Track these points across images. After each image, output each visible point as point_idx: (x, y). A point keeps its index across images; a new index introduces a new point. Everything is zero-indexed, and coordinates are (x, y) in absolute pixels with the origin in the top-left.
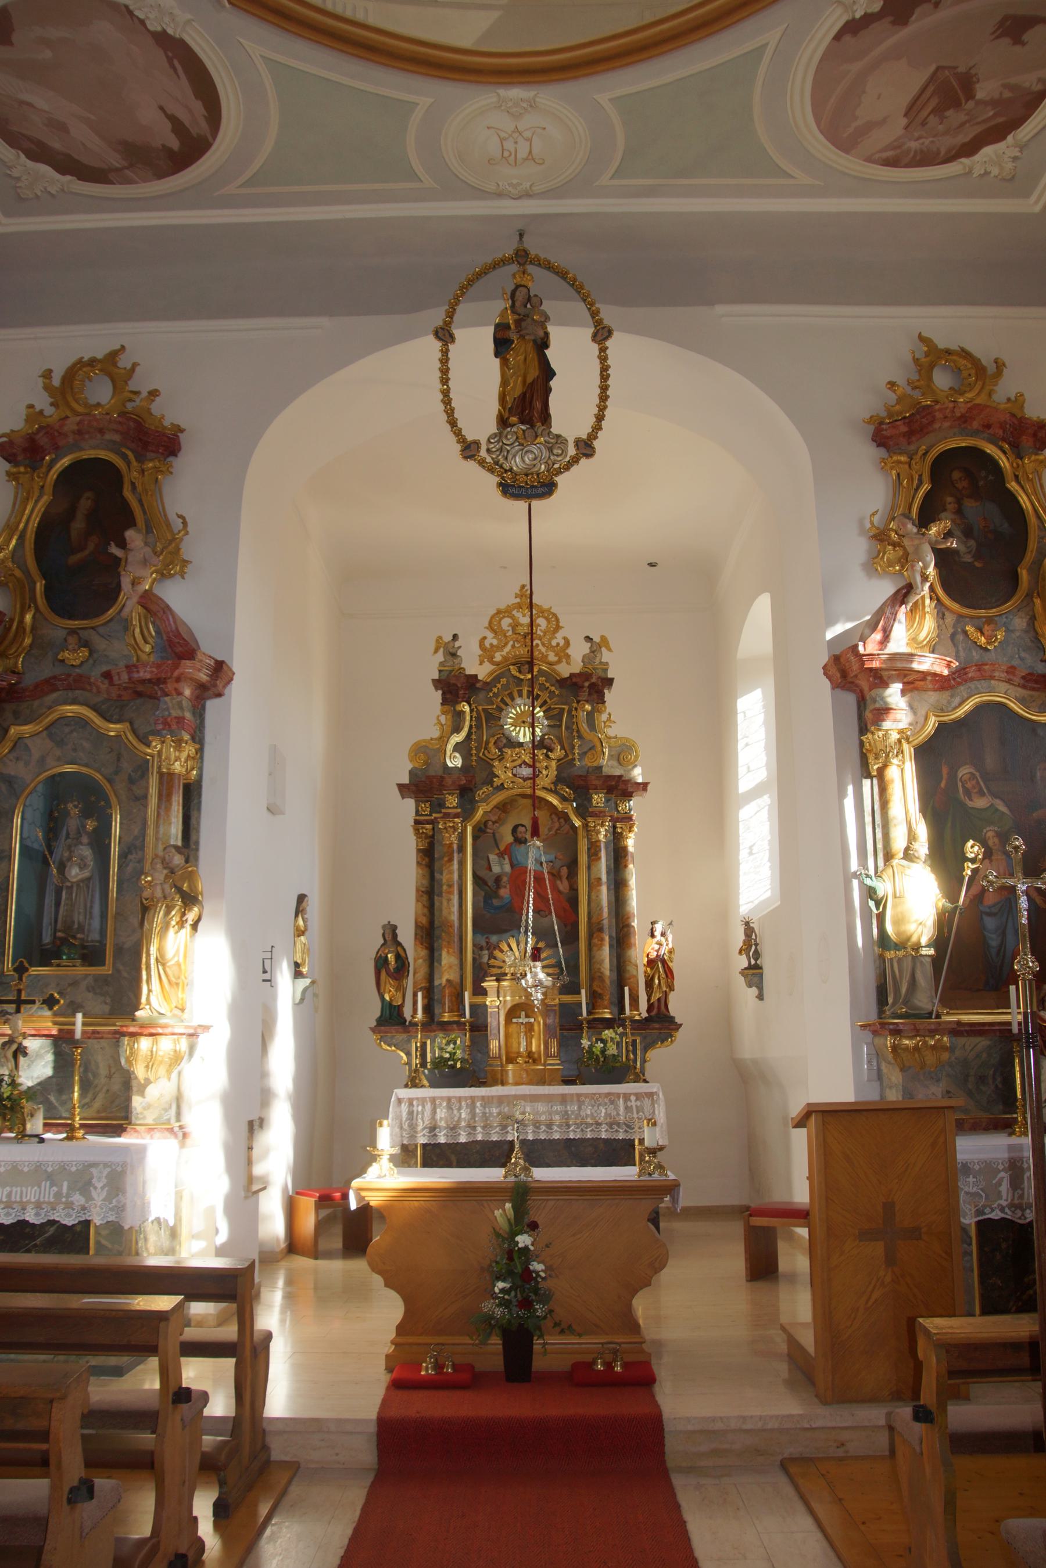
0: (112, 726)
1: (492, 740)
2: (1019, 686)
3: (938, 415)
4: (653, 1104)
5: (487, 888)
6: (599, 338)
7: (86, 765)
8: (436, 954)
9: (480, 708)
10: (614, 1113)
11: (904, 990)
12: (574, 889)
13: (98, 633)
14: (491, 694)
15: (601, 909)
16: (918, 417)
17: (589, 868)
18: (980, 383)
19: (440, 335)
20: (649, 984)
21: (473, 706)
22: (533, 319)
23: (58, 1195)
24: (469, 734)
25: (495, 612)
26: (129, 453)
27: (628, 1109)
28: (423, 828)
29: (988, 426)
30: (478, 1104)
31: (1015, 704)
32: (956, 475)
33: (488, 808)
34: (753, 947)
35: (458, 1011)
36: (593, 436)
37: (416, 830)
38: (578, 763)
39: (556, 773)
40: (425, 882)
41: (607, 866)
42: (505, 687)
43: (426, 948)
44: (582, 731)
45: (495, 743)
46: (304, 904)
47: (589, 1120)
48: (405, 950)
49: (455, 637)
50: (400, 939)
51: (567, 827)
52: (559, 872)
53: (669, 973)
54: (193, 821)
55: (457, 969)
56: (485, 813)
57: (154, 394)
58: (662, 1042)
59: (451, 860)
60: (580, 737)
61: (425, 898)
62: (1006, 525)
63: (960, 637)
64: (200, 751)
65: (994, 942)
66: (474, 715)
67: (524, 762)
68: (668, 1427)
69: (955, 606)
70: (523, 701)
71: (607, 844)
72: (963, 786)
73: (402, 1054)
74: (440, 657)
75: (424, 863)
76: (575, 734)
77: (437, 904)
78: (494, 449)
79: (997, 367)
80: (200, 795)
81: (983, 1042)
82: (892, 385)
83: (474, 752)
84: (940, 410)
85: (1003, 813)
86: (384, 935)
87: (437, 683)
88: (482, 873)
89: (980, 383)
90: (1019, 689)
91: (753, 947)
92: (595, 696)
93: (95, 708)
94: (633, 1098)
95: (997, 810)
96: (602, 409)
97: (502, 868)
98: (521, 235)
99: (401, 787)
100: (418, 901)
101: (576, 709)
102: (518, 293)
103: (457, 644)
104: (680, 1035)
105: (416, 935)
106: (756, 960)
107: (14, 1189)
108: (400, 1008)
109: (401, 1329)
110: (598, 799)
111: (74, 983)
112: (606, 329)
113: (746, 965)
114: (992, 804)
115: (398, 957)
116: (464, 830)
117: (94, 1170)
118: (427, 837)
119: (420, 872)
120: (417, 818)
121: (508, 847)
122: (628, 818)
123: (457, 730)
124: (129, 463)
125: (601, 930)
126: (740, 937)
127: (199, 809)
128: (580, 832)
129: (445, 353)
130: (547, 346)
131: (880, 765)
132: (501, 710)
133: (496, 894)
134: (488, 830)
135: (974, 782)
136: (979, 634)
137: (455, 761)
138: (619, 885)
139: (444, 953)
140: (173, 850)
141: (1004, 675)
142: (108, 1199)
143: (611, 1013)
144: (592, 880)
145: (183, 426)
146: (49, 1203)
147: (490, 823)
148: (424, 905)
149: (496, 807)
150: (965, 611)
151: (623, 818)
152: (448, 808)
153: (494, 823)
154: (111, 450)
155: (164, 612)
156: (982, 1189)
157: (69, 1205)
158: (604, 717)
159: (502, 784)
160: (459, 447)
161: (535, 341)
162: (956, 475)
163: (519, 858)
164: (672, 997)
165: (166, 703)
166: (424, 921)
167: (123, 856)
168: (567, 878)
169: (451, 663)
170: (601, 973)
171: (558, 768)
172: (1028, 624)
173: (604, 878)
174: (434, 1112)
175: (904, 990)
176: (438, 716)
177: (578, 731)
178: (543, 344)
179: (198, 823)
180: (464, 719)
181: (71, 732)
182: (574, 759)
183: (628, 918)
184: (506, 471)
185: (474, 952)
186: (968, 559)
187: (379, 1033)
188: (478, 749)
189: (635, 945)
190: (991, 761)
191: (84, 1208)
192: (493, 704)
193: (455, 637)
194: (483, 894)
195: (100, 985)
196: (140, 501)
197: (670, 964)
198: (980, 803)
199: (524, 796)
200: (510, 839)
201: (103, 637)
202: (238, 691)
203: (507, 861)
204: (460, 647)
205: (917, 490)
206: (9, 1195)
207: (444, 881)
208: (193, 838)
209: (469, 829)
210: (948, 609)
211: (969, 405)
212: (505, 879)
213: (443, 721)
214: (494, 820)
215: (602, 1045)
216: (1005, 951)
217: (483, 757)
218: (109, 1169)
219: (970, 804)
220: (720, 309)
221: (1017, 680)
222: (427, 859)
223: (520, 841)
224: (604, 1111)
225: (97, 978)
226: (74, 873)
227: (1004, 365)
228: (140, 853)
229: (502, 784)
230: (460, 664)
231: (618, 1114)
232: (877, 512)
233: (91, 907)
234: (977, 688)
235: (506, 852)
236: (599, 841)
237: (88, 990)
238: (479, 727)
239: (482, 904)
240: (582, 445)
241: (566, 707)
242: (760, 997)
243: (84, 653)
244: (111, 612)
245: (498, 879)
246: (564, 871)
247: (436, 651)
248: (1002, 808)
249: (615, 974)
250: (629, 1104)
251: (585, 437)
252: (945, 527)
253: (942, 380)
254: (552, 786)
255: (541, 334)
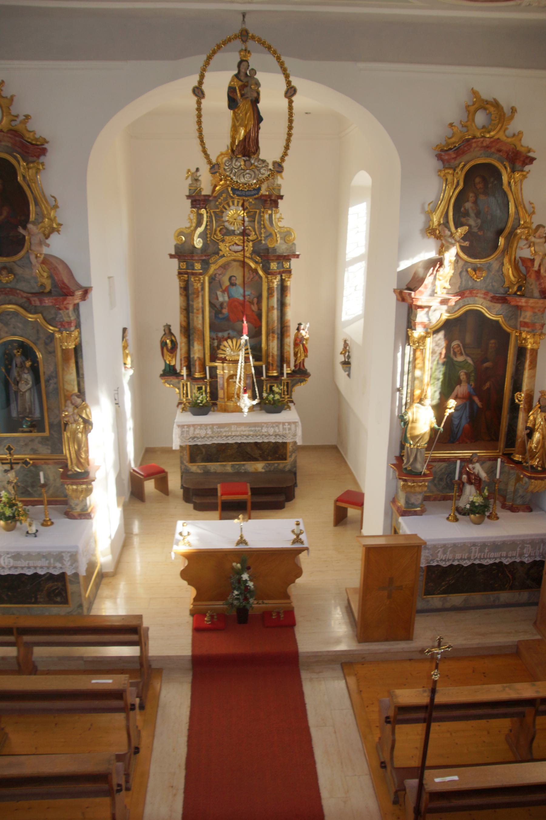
0: (31, 316)
1: (219, 229)
2: (489, 300)
3: (474, 145)
4: (296, 426)
5: (216, 309)
6: (289, 95)
7: (21, 336)
8: (191, 342)
9: (212, 211)
10: (277, 431)
11: (411, 460)
12: (260, 309)
13: (17, 265)
14: (217, 203)
15: (274, 322)
16: (462, 147)
17: (268, 299)
18: (500, 125)
19: (196, 92)
20: (296, 354)
21: (208, 210)
22: (251, 88)
23: (50, 563)
24: (207, 225)
25: (219, 153)
26: (18, 156)
27: (284, 429)
28: (182, 276)
29: (499, 151)
30: (215, 427)
31: (484, 310)
32: (477, 180)
33: (217, 267)
34: (347, 354)
35: (203, 372)
36: (283, 159)
37: (179, 278)
38: (263, 242)
39: (252, 249)
40: (184, 304)
41: (278, 298)
42: (225, 199)
43: (186, 338)
44: (266, 225)
45: (220, 231)
46: (126, 332)
47: (266, 434)
48: (175, 337)
49: (197, 170)
50: (173, 331)
51: (257, 277)
52: (253, 301)
53: (305, 350)
54: (80, 364)
55: (202, 351)
56: (215, 270)
57: (27, 117)
58: (301, 382)
59: (198, 296)
60: (265, 228)
61: (185, 312)
62: (498, 211)
63: (464, 273)
64: (80, 333)
65: (456, 422)
66: (209, 215)
67: (236, 243)
68: (300, 655)
69: (465, 257)
70: (235, 208)
71: (277, 288)
72: (453, 351)
73: (177, 390)
74: (189, 181)
75: (183, 294)
76: (262, 226)
77: (191, 317)
78: (228, 170)
79: (512, 112)
80: (81, 351)
81: (444, 465)
82: (451, 125)
83: (209, 236)
84: (475, 142)
85: (470, 364)
86: (164, 330)
87: (189, 197)
88: (214, 301)
89: (500, 125)
90: (489, 302)
91: (347, 354)
92: (273, 205)
93: (21, 306)
94: (287, 424)
95: (467, 362)
96: (288, 140)
97: (224, 299)
98: (244, 16)
99: (171, 256)
100: (181, 313)
101: (263, 212)
102: (242, 66)
103: (198, 174)
104: (309, 379)
105: (181, 331)
106: (348, 359)
107: (30, 562)
108: (174, 366)
109: (195, 599)
110: (274, 266)
111: (32, 440)
112: (293, 89)
113: (343, 360)
114: (465, 360)
115: (172, 341)
116: (204, 280)
117: (64, 554)
118: (185, 281)
119: (182, 299)
120: (179, 270)
121: (227, 288)
122: (289, 272)
123: (199, 224)
124: (19, 162)
125: (273, 332)
126: (340, 347)
127: (82, 358)
128: (264, 280)
129: (199, 103)
130: (258, 102)
131: (415, 348)
132: (223, 212)
133: (221, 313)
134: (217, 279)
135: (458, 349)
136: (474, 273)
137: (198, 243)
138: (282, 305)
139: (196, 344)
140: (76, 398)
141: (482, 296)
142: (71, 565)
143: (277, 372)
144: (269, 307)
145: (47, 139)
146: (46, 567)
147: (217, 275)
148: (185, 317)
149: (220, 267)
150: (469, 260)
151: (286, 271)
152: (196, 270)
153: (220, 275)
154: (7, 153)
155: (54, 270)
156: (431, 555)
157: (55, 567)
158: (278, 216)
159: (224, 255)
160: (208, 167)
161: (252, 101)
162: (477, 180)
163: (232, 293)
164: (306, 360)
165: (60, 314)
166: (184, 324)
167: (47, 381)
168: (257, 304)
169: (195, 185)
170: (273, 353)
171: (253, 247)
172: (499, 268)
173: (276, 306)
174: (194, 430)
175: (411, 460)
176: (189, 215)
177: (264, 225)
178: (256, 101)
179: (82, 365)
180: (203, 218)
181: (11, 318)
182: (261, 240)
183: (287, 323)
184: (234, 181)
185: (210, 341)
186: (475, 230)
187: (165, 379)
188: (211, 234)
189: (289, 336)
190: (469, 339)
191: (61, 568)
192: (218, 209)
193: (197, 170)
194: (214, 311)
195: (44, 441)
196: (29, 186)
197: (306, 346)
198: (460, 359)
199: (234, 260)
200: (227, 283)
201: (19, 266)
202: (95, 295)
203: (226, 295)
204: (200, 176)
205: (455, 189)
206: (28, 564)
207: (195, 306)
208: (81, 372)
209: (207, 278)
210: (460, 258)
211: (492, 140)
212: (225, 304)
213: (192, 218)
214: (219, 273)
215: (273, 396)
216: (460, 426)
217: (213, 239)
218: (69, 554)
219: (455, 359)
220: (361, 65)
221: (489, 298)
222: (185, 292)
223: (233, 284)
224: (273, 430)
225: (43, 438)
226: (24, 387)
227: (516, 111)
228: (55, 380)
229: (224, 255)
230: (200, 185)
231: (279, 431)
232: (432, 202)
233: (34, 401)
234: (468, 301)
235: (226, 290)
236: (273, 287)
237: (40, 443)
238: (211, 221)
239: (213, 317)
240: (276, 165)
241: (258, 211)
242: (349, 375)
243: (12, 277)
244: (22, 253)
245: (222, 304)
246: (255, 300)
247: (187, 178)
248: (470, 361)
249: (279, 352)
250: (285, 427)
251: (279, 160)
252: (465, 230)
253: (480, 118)
254: (250, 256)
255: (255, 95)
